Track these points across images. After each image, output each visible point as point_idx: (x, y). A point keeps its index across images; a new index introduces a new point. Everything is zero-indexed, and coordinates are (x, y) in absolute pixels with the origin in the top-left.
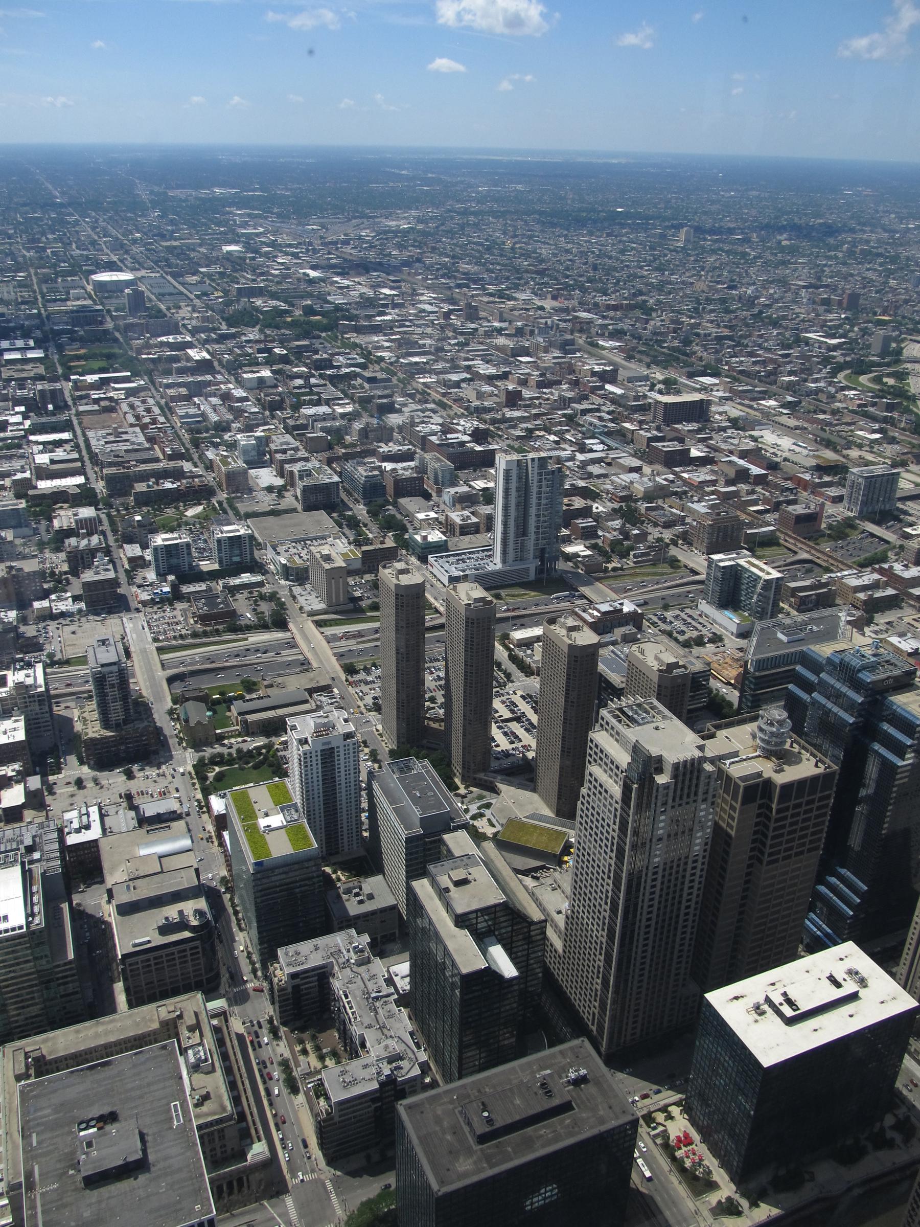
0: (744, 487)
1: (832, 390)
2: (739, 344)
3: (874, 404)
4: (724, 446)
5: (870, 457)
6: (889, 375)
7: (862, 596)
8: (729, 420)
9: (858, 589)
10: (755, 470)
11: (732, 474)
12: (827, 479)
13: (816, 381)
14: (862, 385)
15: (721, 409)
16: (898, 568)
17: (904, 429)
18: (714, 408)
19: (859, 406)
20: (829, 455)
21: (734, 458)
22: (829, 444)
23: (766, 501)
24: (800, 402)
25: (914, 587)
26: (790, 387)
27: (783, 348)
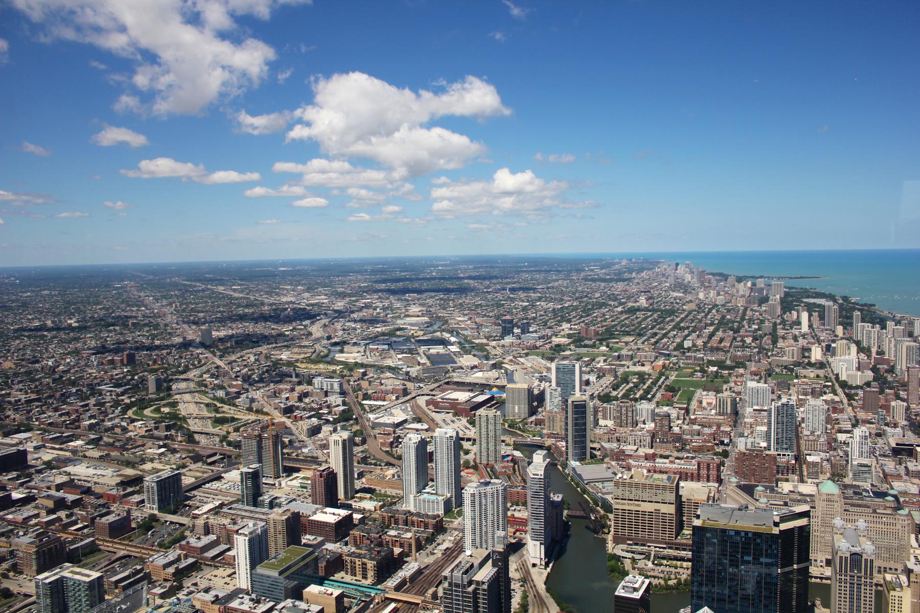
0: (62, 514)
1: (124, 424)
2: (46, 404)
3: (157, 428)
4: (43, 485)
5: (160, 466)
6: (164, 406)
7: (171, 570)
8: (45, 463)
9: (166, 566)
10: (71, 497)
11: (50, 504)
12: (129, 490)
13: (111, 419)
14: (147, 417)
15: (36, 456)
16: (193, 541)
17: (181, 442)
18: (29, 457)
19: (146, 431)
20: (130, 472)
21: (53, 492)
22: (128, 464)
23: (84, 519)
24: (101, 438)
25: (207, 551)
26: (91, 427)
27: (83, 400)
